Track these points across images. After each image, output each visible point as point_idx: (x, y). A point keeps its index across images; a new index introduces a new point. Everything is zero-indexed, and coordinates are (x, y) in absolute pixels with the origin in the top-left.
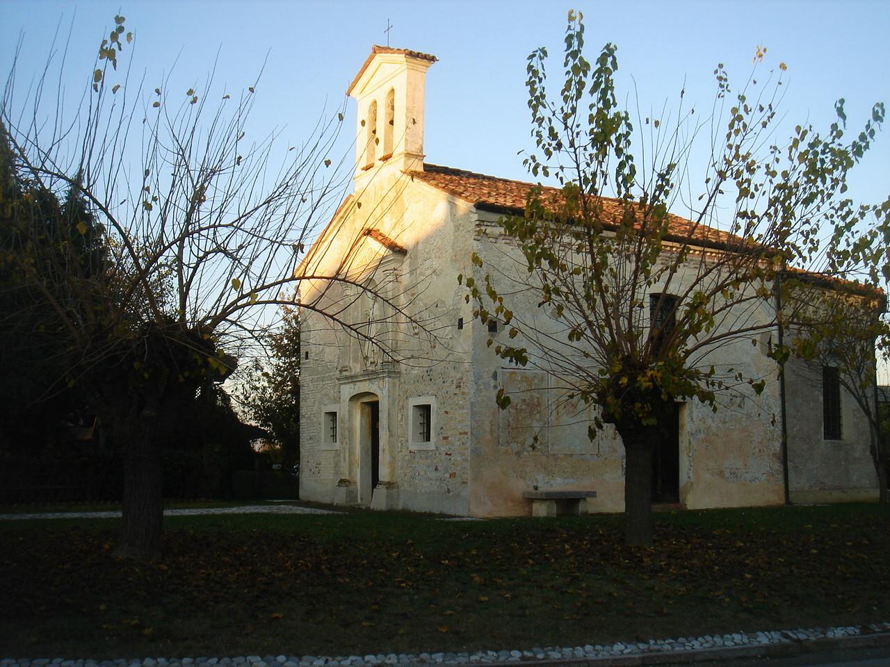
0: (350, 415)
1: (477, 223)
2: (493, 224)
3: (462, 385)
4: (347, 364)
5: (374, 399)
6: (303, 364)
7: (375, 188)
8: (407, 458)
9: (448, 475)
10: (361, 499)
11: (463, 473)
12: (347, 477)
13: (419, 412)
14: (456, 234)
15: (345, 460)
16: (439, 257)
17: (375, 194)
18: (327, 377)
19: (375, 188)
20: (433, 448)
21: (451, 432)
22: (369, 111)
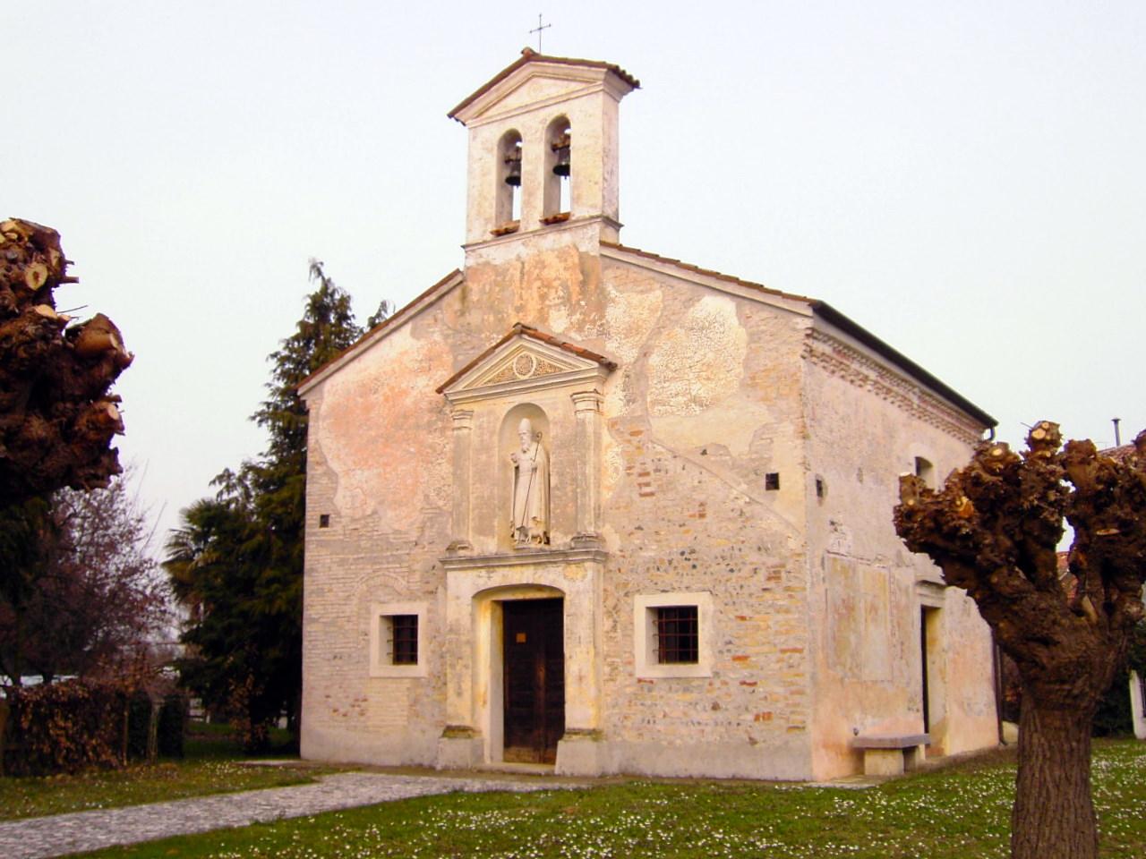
0: (473, 621)
1: (809, 332)
2: (821, 337)
3: (783, 575)
4: (462, 536)
5: (557, 595)
6: (315, 534)
7: (523, 263)
8: (628, 690)
9: (749, 717)
10: (492, 758)
11: (792, 713)
12: (467, 722)
13: (387, 625)
14: (753, 346)
15: (459, 694)
16: (708, 379)
17: (522, 273)
18: (387, 557)
19: (523, 263)
20: (708, 673)
21: (757, 649)
22: (618, 159)
